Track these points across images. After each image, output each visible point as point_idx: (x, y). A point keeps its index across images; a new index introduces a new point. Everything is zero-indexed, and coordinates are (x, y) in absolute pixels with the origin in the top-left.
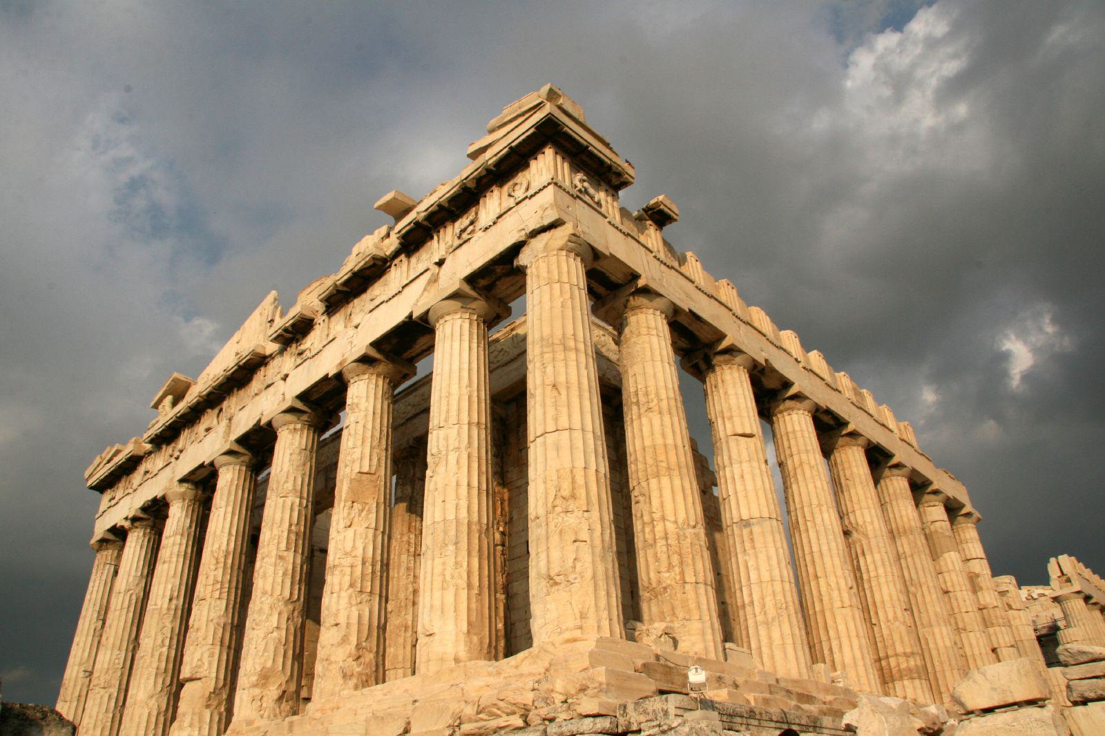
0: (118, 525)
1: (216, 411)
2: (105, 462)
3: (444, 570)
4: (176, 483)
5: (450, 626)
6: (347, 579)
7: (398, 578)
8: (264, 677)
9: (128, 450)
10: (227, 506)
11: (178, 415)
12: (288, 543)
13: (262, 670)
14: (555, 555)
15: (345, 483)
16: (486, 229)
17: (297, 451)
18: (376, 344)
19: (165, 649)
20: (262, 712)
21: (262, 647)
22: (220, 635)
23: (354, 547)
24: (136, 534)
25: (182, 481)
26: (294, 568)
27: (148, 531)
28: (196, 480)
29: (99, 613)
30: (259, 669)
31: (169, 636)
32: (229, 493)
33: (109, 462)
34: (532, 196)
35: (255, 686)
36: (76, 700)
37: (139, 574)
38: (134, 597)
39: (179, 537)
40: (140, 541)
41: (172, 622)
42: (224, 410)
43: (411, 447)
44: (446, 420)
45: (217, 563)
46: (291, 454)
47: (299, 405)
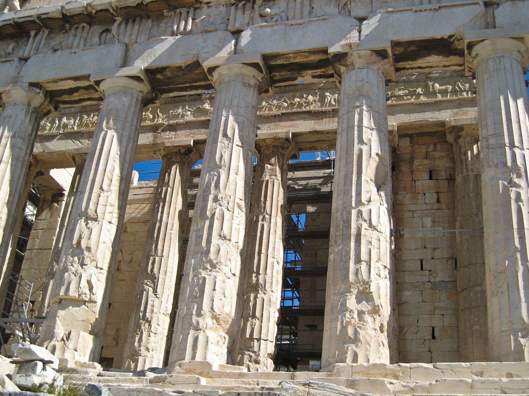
1: (98, 29)
4: (26, 85)
11: (43, 17)
18: (395, 44)
25: (32, 85)
32: (126, 117)
46: (246, 107)
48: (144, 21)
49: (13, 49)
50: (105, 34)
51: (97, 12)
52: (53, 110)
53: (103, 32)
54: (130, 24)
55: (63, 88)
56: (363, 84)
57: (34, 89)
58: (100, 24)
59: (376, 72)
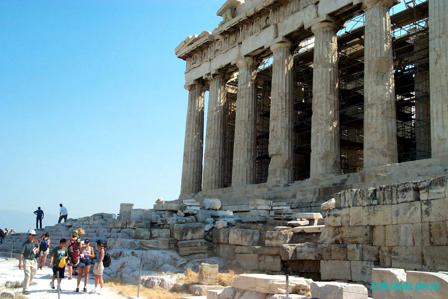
1: (264, 18)
2: (187, 44)
4: (244, 57)
6: (380, 110)
8: (326, 156)
11: (240, 21)
12: (331, 91)
13: (325, 152)
19: (249, 140)
20: (327, 171)
21: (325, 141)
22: (288, 134)
24: (216, 82)
25: (246, 56)
26: (334, 103)
27: (221, 80)
28: (254, 55)
29: (196, 121)
30: (324, 152)
31: (250, 133)
33: (190, 44)
41: (251, 127)
42: (270, 18)
44: (443, 33)
45: (282, 99)
48: (280, 7)
49: (235, 39)
50: (268, 20)
51: (260, 11)
52: (260, 62)
53: (267, 19)
54: (275, 12)
55: (259, 53)
56: (371, 18)
57: (247, 57)
58: (264, 16)
59: (378, 8)
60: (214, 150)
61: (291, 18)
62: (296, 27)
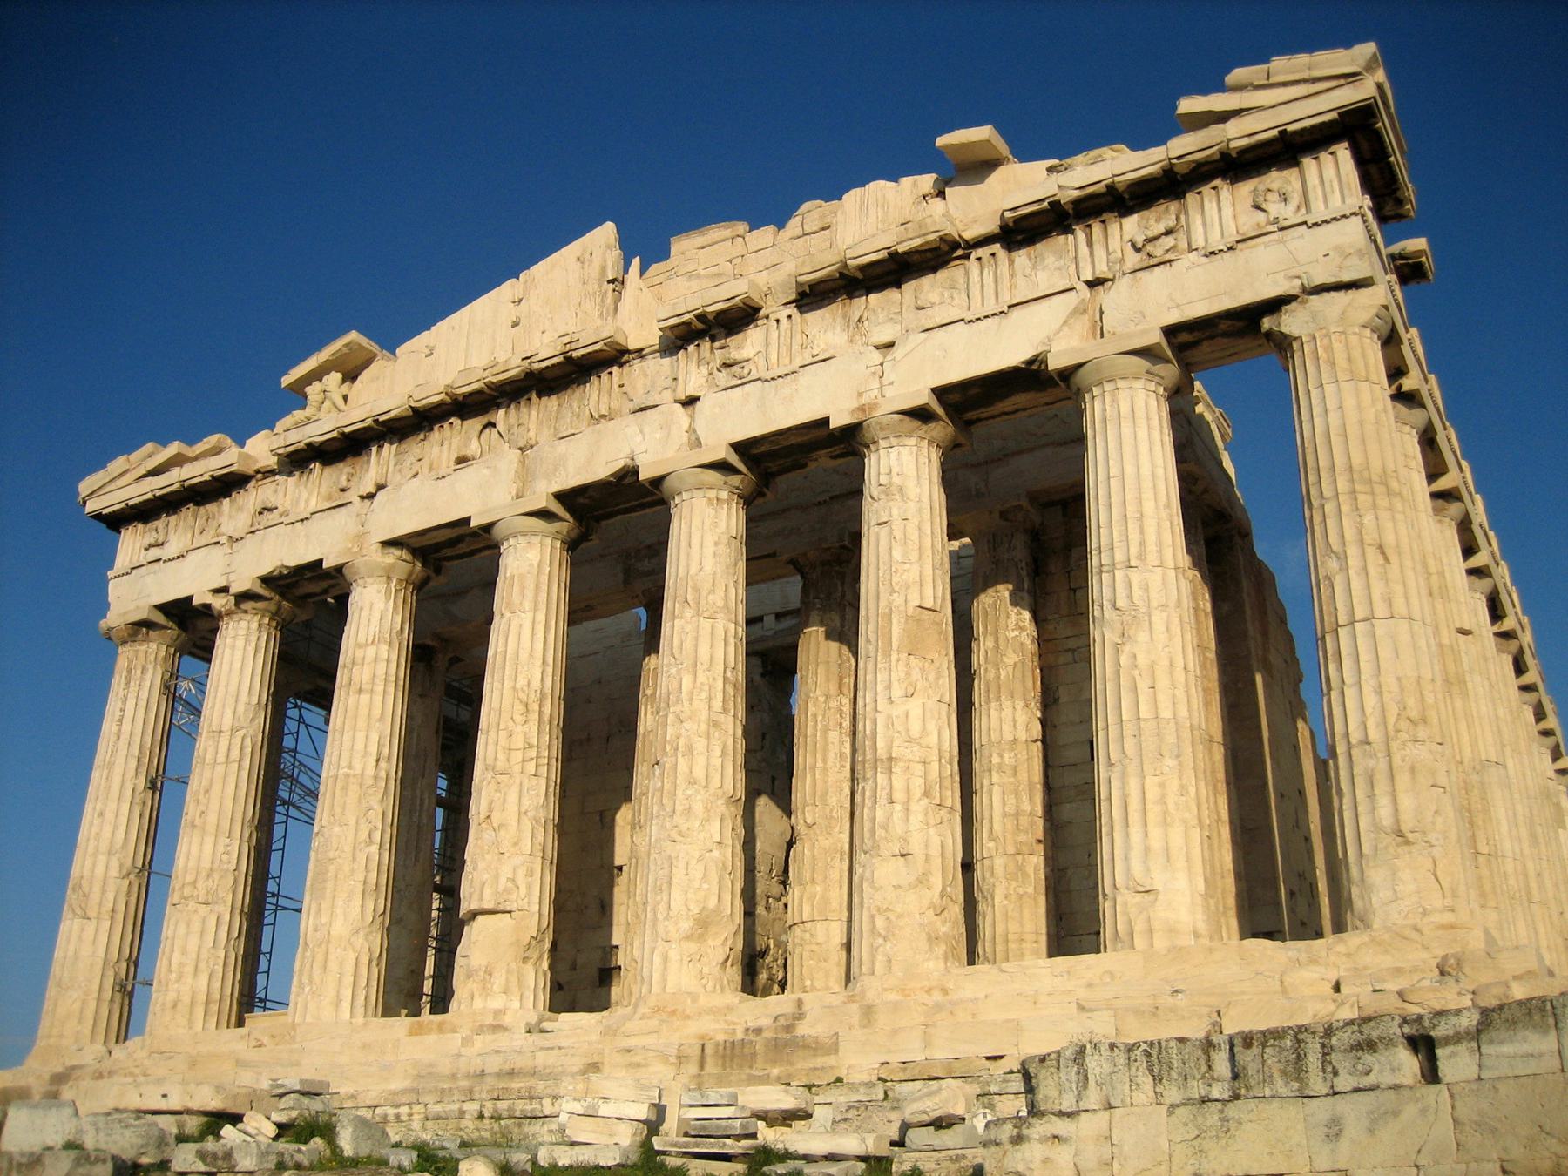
0: (195, 602)
3: (1163, 796)
5: (1181, 882)
7: (825, 769)
9: (230, 458)
10: (535, 609)
11: (381, 418)
14: (1406, 802)
15: (894, 621)
16: (1213, 253)
17: (725, 539)
19: (374, 849)
22: (540, 839)
23: (924, 730)
25: (388, 544)
27: (266, 620)
30: (696, 911)
34: (1316, 224)
35: (688, 938)
36: (107, 917)
37: (255, 700)
38: (248, 742)
39: (384, 648)
40: (254, 638)
43: (843, 547)
46: (716, 544)
47: (734, 460)
60: (216, 876)
61: (587, 435)
62: (601, 470)
